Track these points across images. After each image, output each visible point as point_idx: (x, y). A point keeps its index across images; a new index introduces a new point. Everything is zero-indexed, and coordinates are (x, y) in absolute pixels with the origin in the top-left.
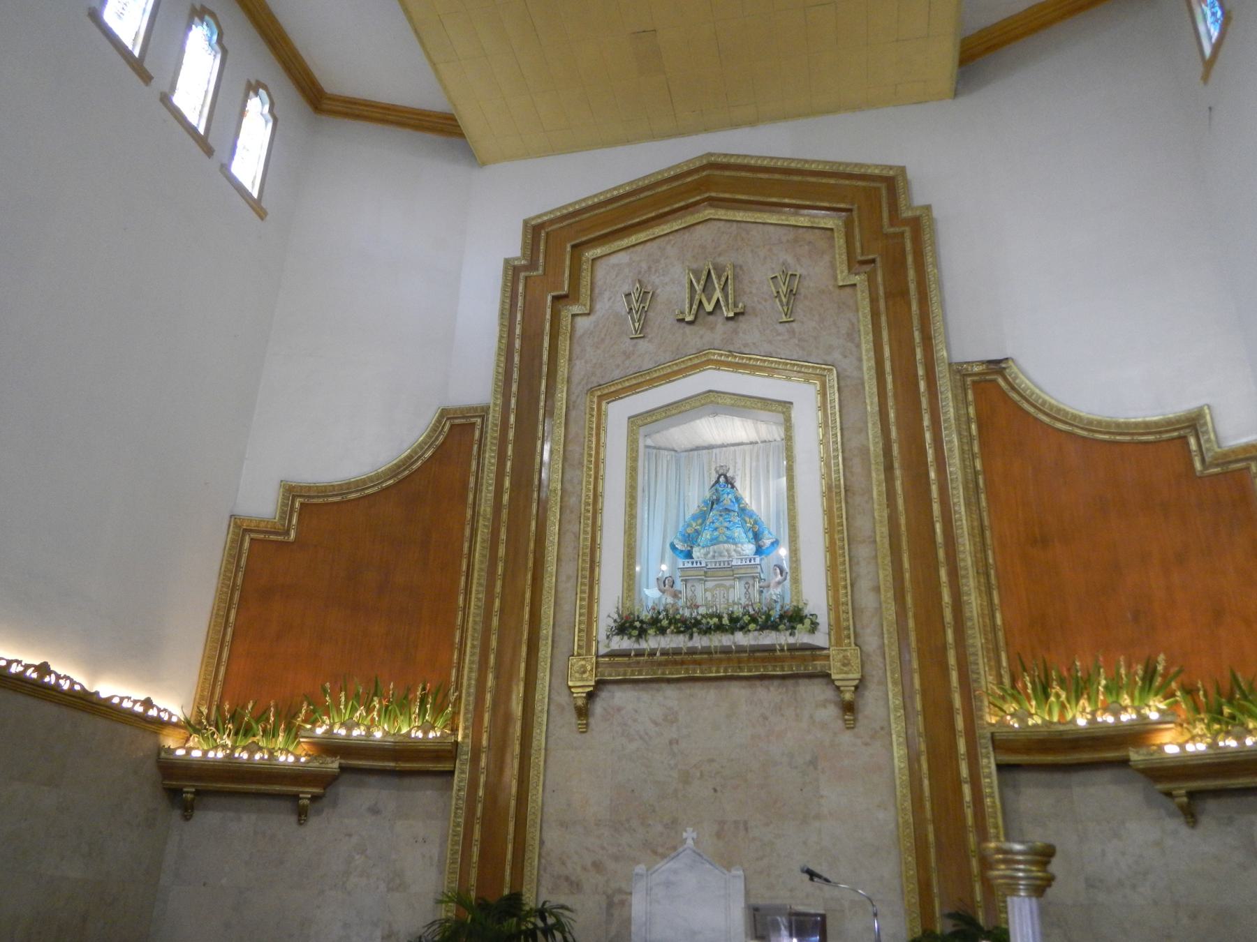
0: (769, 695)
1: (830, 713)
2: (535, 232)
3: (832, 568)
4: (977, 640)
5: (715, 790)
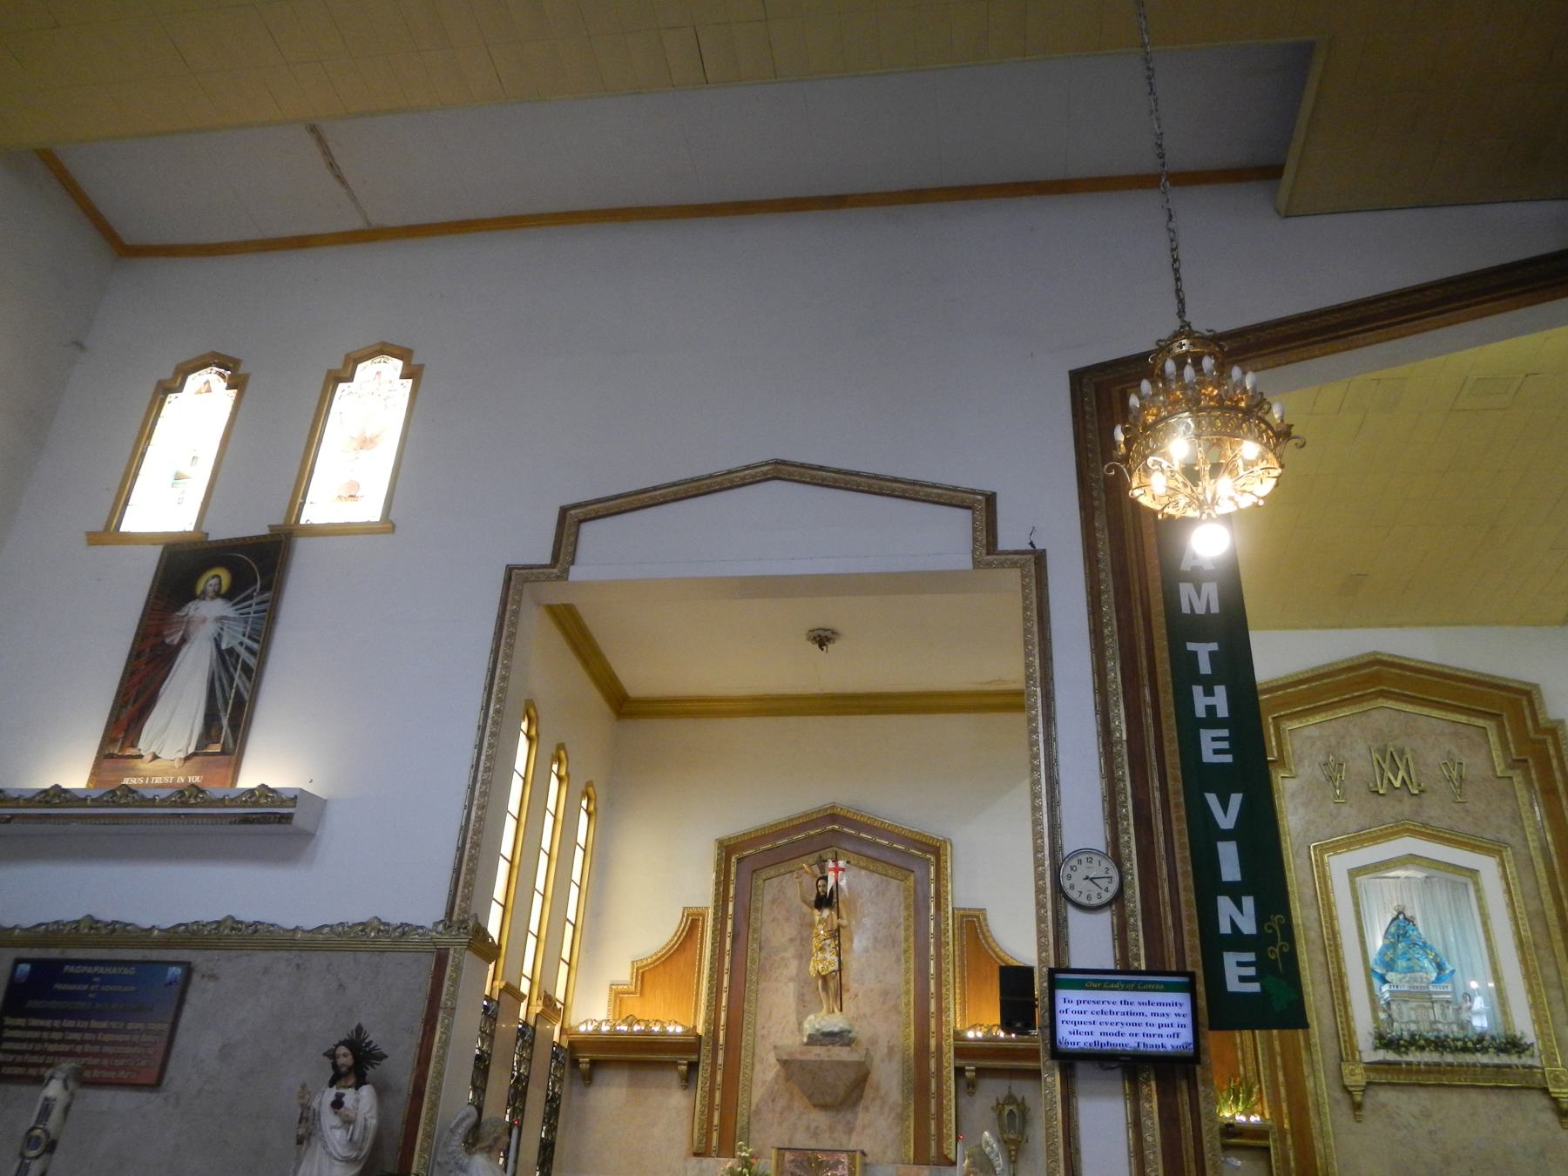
0: (1500, 1101)
5: (1472, 1171)
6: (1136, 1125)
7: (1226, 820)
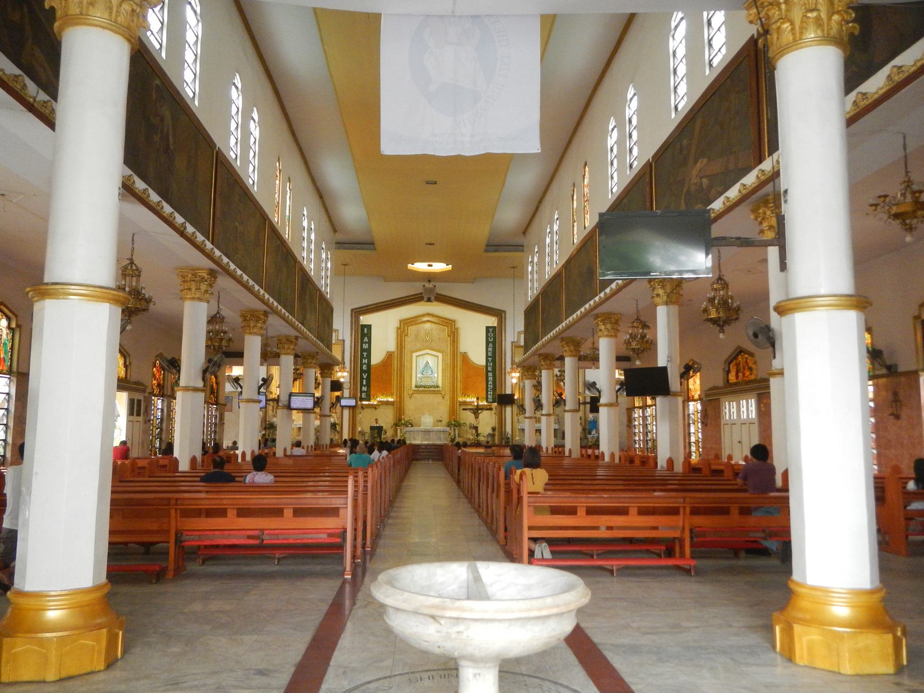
0: (434, 395)
1: (441, 398)
2: (401, 321)
3: (442, 380)
4: (458, 390)
6: (349, 413)
7: (365, 377)
